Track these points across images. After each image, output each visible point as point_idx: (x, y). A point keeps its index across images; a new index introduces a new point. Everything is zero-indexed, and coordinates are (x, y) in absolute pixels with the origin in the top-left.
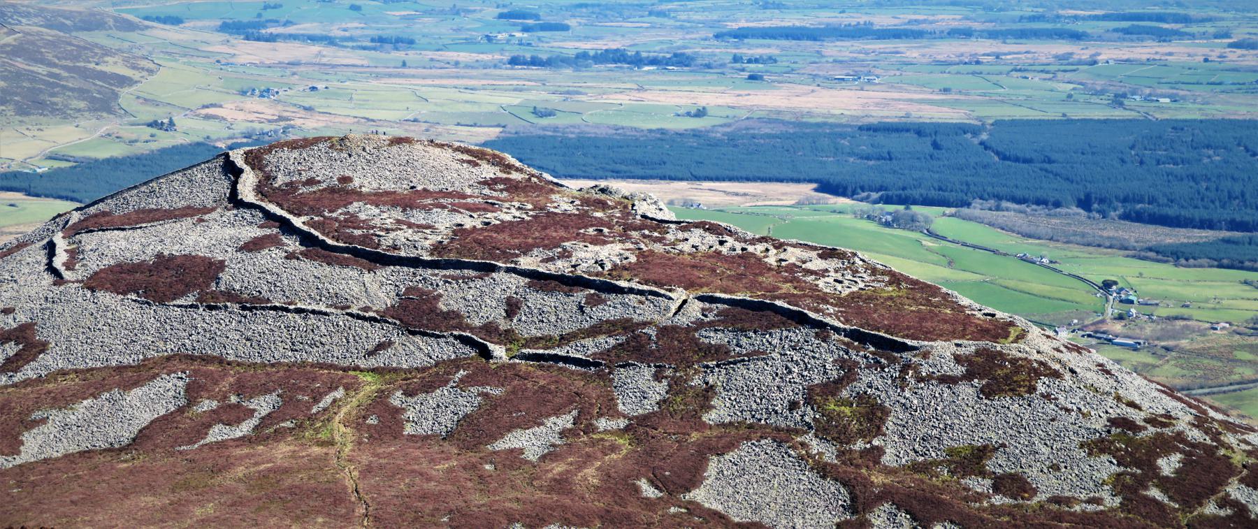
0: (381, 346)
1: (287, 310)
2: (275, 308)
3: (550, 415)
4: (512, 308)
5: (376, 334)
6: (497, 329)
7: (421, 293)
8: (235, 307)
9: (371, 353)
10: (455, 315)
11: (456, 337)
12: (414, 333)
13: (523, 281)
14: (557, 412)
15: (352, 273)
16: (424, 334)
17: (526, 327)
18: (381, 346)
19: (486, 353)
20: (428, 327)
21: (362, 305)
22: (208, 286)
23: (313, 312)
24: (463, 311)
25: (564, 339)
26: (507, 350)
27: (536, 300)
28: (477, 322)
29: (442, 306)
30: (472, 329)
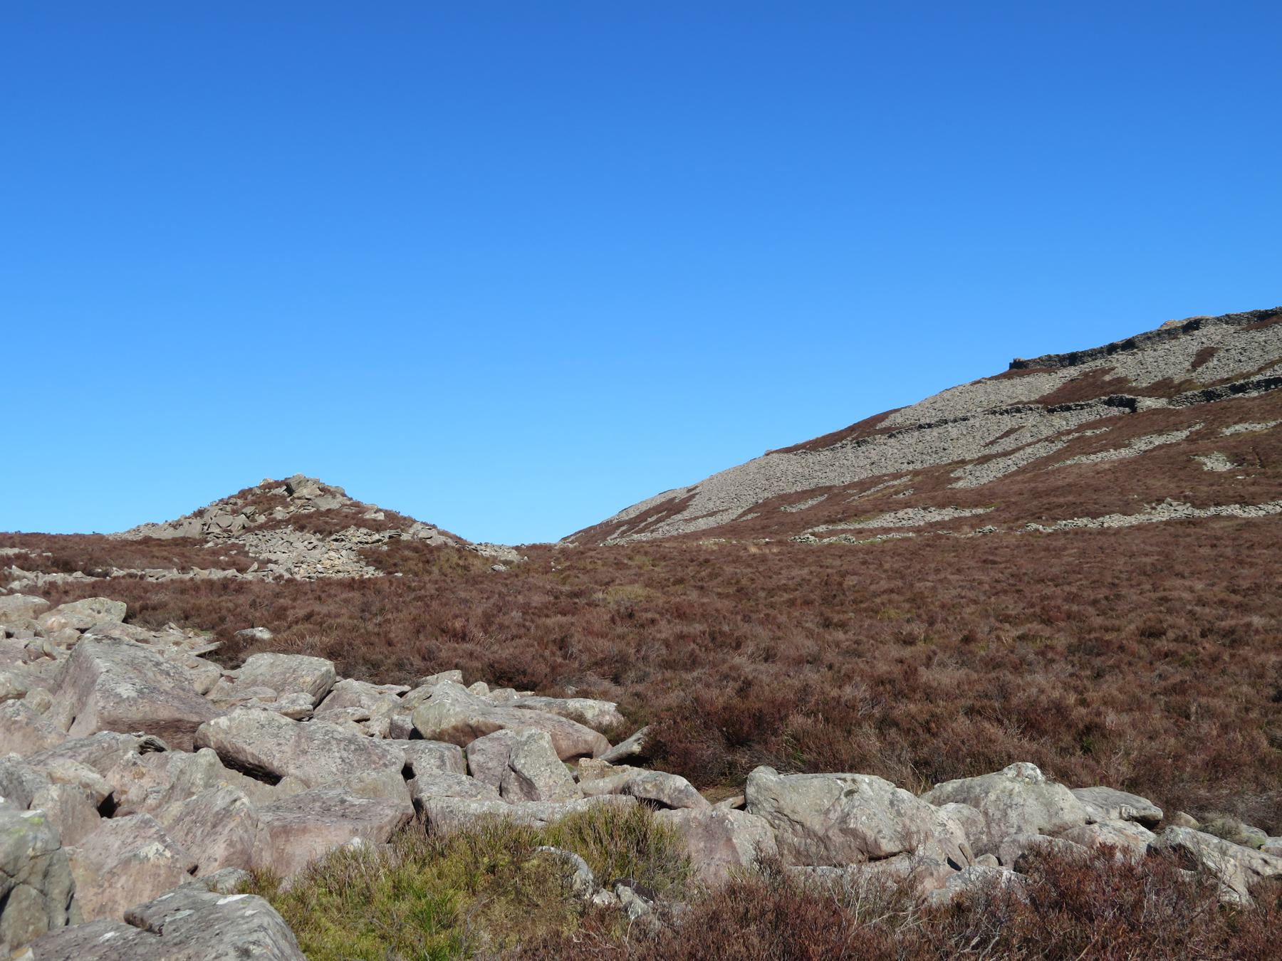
0: (1007, 434)
1: (930, 426)
2: (921, 427)
3: (1145, 434)
4: (1204, 356)
5: (1008, 422)
7: (1086, 375)
8: (881, 439)
9: (992, 443)
10: (1121, 381)
12: (1051, 411)
13: (1231, 329)
14: (1160, 433)
15: (1027, 379)
16: (1069, 409)
17: (1211, 373)
18: (1007, 434)
19: (1131, 404)
22: (875, 425)
23: (955, 421)
24: (1131, 377)
25: (1260, 370)
26: (1169, 403)
27: (1241, 341)
29: (1107, 378)
30: (1131, 391)
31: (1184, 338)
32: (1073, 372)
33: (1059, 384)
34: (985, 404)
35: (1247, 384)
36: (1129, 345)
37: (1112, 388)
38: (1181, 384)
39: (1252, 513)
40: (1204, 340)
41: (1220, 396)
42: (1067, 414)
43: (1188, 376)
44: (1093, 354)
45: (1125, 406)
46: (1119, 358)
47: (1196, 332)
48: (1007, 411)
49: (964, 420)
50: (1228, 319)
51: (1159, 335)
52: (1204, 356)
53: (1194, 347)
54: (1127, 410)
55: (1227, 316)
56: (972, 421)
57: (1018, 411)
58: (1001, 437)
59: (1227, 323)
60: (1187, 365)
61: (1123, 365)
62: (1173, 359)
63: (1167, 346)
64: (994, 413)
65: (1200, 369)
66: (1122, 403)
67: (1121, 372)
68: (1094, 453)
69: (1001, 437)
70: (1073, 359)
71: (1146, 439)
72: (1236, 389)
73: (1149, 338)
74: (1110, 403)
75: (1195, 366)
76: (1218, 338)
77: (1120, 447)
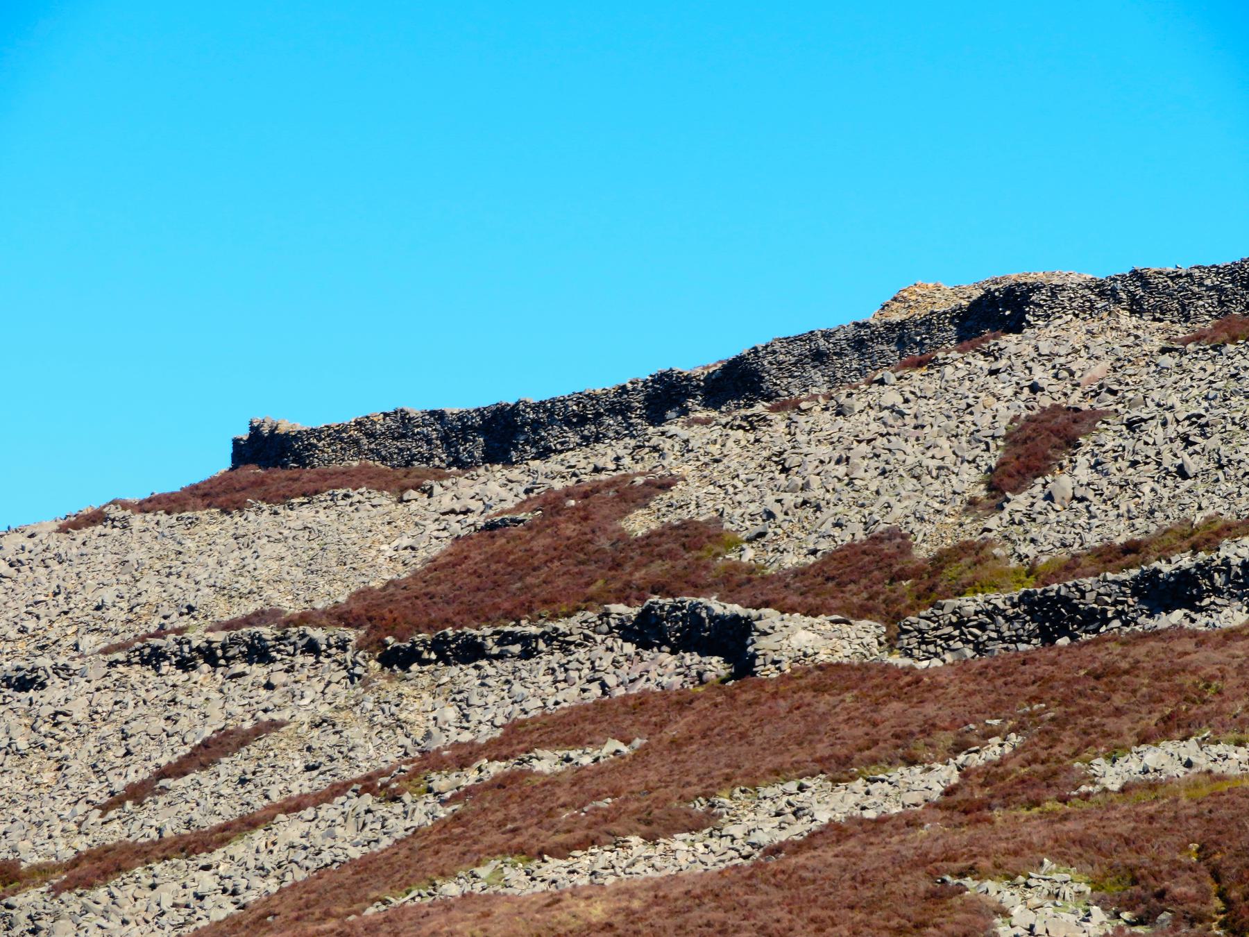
0: (205, 754)
3: (778, 774)
4: (1037, 447)
6: (905, 548)
9: (138, 793)
10: (695, 538)
11: (626, 632)
12: (398, 660)
14: (840, 769)
15: (302, 515)
16: (471, 652)
17: (1060, 521)
18: (205, 754)
19: (731, 640)
20: (482, 618)
21: (251, 607)
26: (891, 644)
28: (791, 560)
29: (639, 523)
30: (735, 582)
31: (960, 366)
32: (496, 489)
33: (434, 544)
34: (116, 615)
35: (1205, 570)
36: (737, 383)
37: (658, 568)
38: (940, 561)
39: (687, 855)
40: (1041, 375)
41: (1094, 618)
42: (464, 675)
43: (970, 531)
44: (585, 417)
45: (706, 650)
46: (697, 433)
47: (1010, 342)
48: (209, 655)
49: (24, 684)
50: (1141, 293)
51: (859, 344)
52: (1037, 447)
53: (1001, 409)
54: (716, 666)
55: (1138, 275)
56: (55, 692)
57: (258, 653)
58: (178, 770)
59: (1136, 307)
60: (970, 481)
61: (709, 472)
62: (912, 453)
63: (891, 397)
64: (154, 658)
65: (1019, 502)
66: (697, 635)
67: (695, 498)
68: (562, 852)
69: (178, 770)
70: (502, 433)
71: (776, 793)
72: (1162, 593)
73: (819, 357)
74: (645, 632)
75: (999, 485)
76: (1099, 370)
77: (670, 831)
